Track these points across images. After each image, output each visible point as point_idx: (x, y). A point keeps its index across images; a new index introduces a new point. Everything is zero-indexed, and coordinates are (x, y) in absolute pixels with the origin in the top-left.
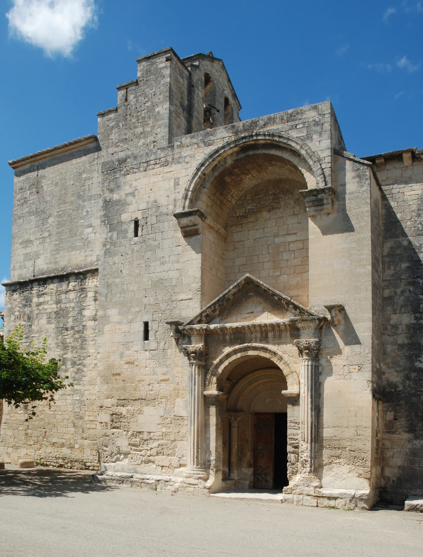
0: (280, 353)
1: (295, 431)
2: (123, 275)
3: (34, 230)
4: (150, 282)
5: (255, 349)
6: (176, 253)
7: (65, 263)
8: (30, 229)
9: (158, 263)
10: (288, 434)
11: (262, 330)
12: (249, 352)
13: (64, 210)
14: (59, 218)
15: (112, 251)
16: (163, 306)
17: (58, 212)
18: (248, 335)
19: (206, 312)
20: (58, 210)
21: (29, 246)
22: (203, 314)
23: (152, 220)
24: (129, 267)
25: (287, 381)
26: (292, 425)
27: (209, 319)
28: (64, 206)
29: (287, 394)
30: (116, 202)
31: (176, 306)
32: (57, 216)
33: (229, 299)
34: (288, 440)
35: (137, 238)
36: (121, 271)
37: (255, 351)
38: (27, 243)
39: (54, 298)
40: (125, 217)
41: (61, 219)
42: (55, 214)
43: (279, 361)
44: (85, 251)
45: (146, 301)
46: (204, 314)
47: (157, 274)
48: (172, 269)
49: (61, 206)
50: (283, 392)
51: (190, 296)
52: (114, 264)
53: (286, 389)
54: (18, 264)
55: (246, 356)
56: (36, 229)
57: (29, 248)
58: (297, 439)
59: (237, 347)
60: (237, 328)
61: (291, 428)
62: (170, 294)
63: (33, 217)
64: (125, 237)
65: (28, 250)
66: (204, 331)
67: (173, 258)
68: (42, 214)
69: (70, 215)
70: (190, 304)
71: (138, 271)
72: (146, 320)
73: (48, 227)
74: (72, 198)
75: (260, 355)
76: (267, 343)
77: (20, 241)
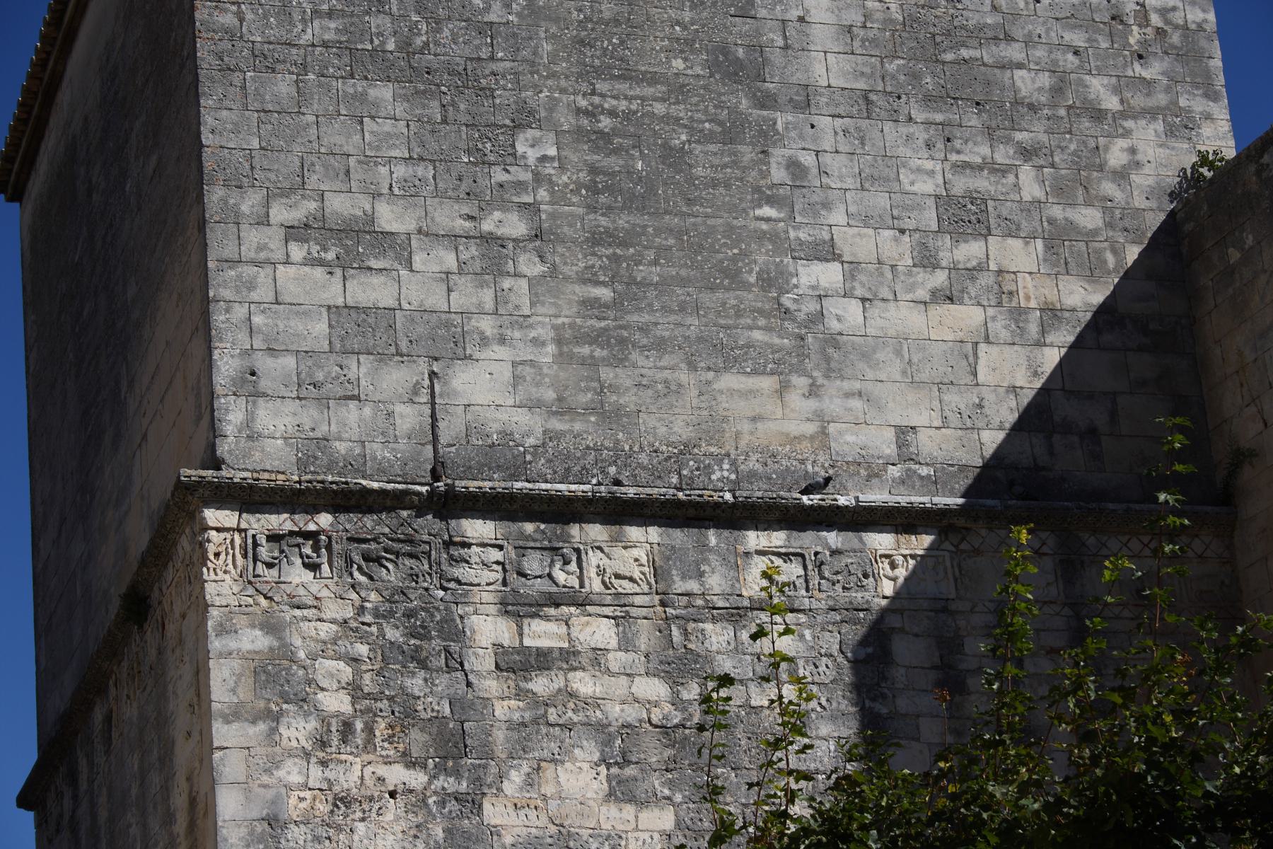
3: (401, 171)
8: (368, 161)
13: (629, 115)
14: (596, 149)
20: (583, 103)
21: (373, 263)
28: (623, 87)
32: (579, 132)
39: (646, 636)
41: (614, 163)
42: (566, 121)
49: (602, 86)
54: (290, 362)
57: (376, 280)
65: (372, 290)
73: (520, 186)
74: (678, 64)
77: (281, 213)
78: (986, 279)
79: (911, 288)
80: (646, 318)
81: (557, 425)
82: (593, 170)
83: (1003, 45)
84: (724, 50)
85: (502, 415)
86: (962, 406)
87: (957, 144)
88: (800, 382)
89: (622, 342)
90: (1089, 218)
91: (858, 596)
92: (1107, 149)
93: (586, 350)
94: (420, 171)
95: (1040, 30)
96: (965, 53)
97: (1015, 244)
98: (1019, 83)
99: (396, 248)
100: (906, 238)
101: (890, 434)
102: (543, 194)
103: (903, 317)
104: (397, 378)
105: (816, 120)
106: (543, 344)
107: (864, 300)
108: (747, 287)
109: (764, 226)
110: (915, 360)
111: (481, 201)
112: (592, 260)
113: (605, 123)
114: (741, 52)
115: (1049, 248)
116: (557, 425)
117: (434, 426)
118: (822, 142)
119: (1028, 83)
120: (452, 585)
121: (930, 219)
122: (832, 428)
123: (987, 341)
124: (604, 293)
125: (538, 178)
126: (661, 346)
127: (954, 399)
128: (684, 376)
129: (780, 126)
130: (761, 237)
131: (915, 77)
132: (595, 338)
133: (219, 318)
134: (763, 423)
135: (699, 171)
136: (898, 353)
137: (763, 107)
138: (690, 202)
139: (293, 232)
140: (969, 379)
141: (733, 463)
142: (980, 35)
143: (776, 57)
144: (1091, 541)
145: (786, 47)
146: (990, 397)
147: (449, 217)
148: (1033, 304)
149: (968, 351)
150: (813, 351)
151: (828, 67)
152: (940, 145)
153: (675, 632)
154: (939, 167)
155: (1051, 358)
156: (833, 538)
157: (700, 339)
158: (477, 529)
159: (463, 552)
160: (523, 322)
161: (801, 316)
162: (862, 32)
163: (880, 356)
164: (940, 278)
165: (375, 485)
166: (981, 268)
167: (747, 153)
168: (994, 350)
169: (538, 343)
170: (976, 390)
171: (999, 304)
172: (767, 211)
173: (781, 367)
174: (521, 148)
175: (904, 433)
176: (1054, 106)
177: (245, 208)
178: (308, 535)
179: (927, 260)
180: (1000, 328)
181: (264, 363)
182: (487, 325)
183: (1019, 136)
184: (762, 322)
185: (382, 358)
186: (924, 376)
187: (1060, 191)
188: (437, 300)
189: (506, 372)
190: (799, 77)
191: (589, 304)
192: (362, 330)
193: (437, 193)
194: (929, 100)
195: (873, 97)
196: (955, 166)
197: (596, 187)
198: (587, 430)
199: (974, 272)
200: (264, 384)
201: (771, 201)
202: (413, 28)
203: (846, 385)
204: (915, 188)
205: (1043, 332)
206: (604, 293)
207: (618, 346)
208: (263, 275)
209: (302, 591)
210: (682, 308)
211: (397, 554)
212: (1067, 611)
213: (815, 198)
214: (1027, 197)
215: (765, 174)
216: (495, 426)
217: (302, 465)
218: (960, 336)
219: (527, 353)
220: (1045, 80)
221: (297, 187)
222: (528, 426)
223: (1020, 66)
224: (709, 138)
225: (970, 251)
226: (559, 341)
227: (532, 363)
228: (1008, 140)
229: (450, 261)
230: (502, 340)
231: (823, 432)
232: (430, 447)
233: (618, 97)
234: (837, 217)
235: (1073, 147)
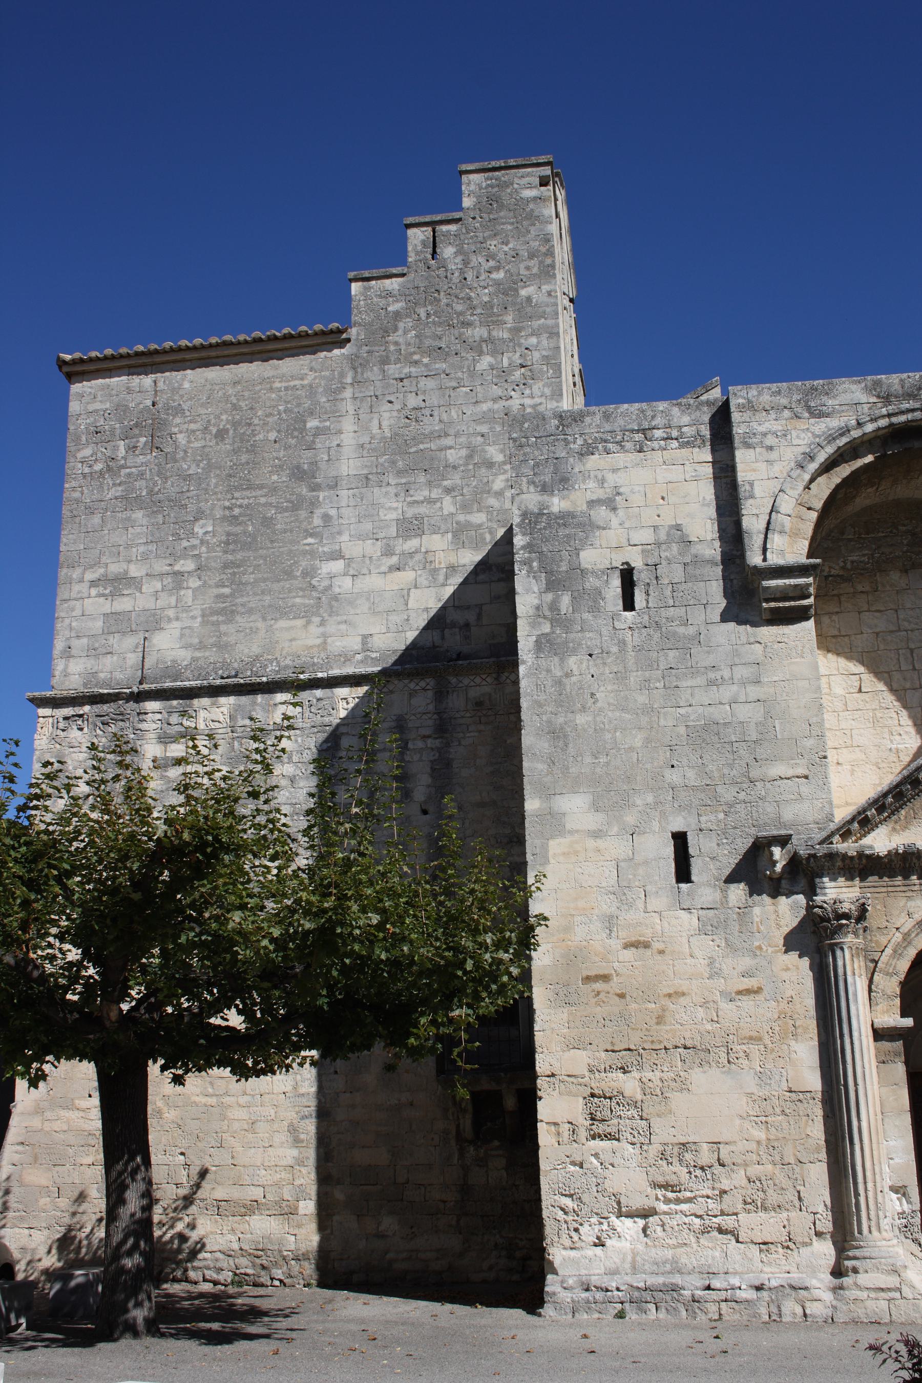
2: (599, 705)
3: (142, 549)
4: (682, 730)
6: (751, 660)
7: (256, 650)
8: (128, 547)
9: (700, 680)
13: (248, 506)
14: (231, 524)
15: (559, 640)
16: (727, 794)
17: (229, 508)
20: (227, 504)
21: (125, 592)
23: (673, 573)
24: (616, 687)
28: (247, 493)
30: (563, 518)
31: (763, 793)
32: (224, 518)
35: (633, 613)
36: (592, 694)
38: (117, 584)
40: (589, 557)
41: (239, 529)
42: (218, 513)
44: (322, 623)
45: (673, 777)
47: (700, 710)
48: (742, 698)
49: (237, 495)
51: (801, 771)
52: (568, 675)
54: (85, 641)
56: (153, 547)
57: (125, 599)
63: (139, 515)
64: (595, 609)
65: (123, 604)
66: (864, 861)
67: (741, 672)
68: (168, 509)
69: (268, 522)
71: (642, 699)
72: (678, 825)
73: (194, 547)
77: (90, 576)
78: (418, 557)
79: (378, 567)
80: (245, 599)
81: (198, 654)
82: (228, 534)
83: (443, 439)
84: (298, 467)
85: (173, 653)
86: (398, 621)
87: (411, 492)
88: (316, 620)
89: (232, 612)
90: (479, 518)
91: (326, 720)
92: (493, 481)
93: (215, 618)
94: (150, 547)
95: (464, 428)
96: (421, 446)
97: (436, 537)
98: (449, 456)
99: (135, 583)
100: (379, 543)
101: (359, 639)
102: (204, 549)
103: (374, 582)
104: (130, 641)
105: (339, 493)
106: (196, 618)
107: (353, 576)
108: (295, 578)
109: (307, 548)
110: (376, 602)
111: (175, 557)
112: (224, 576)
113: (237, 511)
114: (306, 467)
115: (454, 536)
116: (198, 654)
117: (143, 661)
118: (341, 505)
119: (452, 456)
120: (138, 732)
121: (393, 531)
122: (329, 640)
123: (416, 587)
124: (227, 591)
125: (202, 542)
126: (250, 611)
127: (395, 618)
128: (260, 624)
129: (321, 499)
130: (305, 553)
131: (394, 462)
132: (217, 613)
133: (58, 625)
134: (294, 642)
135: (279, 526)
136: (368, 599)
137: (314, 490)
138: (272, 542)
139: (93, 583)
140: (404, 607)
141: (278, 663)
142: (431, 437)
143: (323, 465)
144: (454, 680)
145: (329, 460)
146: (413, 615)
147: (161, 566)
148: (443, 565)
149: (404, 595)
150: (326, 604)
151: (349, 466)
152: (403, 494)
153: (236, 743)
154: (400, 505)
155: (449, 591)
156: (319, 693)
157: (270, 606)
158: (152, 706)
159: (144, 717)
160: (187, 609)
161: (321, 588)
162: (368, 446)
163: (358, 602)
164: (394, 560)
165: (106, 691)
166: (416, 552)
167: (303, 514)
168: (418, 591)
169: (194, 618)
170: (406, 612)
171: (424, 568)
172: (310, 540)
173: (307, 614)
174: (196, 530)
175: (365, 638)
176: (467, 464)
177: (74, 576)
178: (81, 716)
179: (388, 552)
180: (423, 581)
181: (75, 643)
182: (171, 613)
183: (445, 483)
184: (301, 593)
185: (124, 633)
186: (380, 609)
187: (465, 508)
188: (151, 605)
189: (177, 633)
190: (334, 473)
191: (218, 596)
192: (117, 623)
193: (157, 557)
194: (400, 473)
195: (370, 476)
196: (409, 503)
197: (230, 542)
198: (211, 655)
199: (411, 555)
200: (74, 652)
201: (312, 535)
202: (155, 484)
203: (339, 618)
204: (386, 518)
205: (446, 578)
206: (227, 591)
207: (229, 614)
208: (78, 604)
209: (74, 740)
210: (263, 593)
211: (116, 720)
212: (436, 716)
213: (335, 530)
214: (446, 512)
215: (310, 523)
216: (170, 658)
217: (85, 685)
218: (402, 586)
219: (188, 623)
220: (464, 452)
221: (97, 563)
222: (184, 656)
223: (450, 448)
224: (286, 510)
225: (413, 544)
226: (203, 616)
227: (189, 628)
228: (439, 486)
229: (159, 586)
230: (177, 619)
231: (325, 643)
232: (140, 671)
233: (243, 498)
234: (345, 537)
235: (474, 484)
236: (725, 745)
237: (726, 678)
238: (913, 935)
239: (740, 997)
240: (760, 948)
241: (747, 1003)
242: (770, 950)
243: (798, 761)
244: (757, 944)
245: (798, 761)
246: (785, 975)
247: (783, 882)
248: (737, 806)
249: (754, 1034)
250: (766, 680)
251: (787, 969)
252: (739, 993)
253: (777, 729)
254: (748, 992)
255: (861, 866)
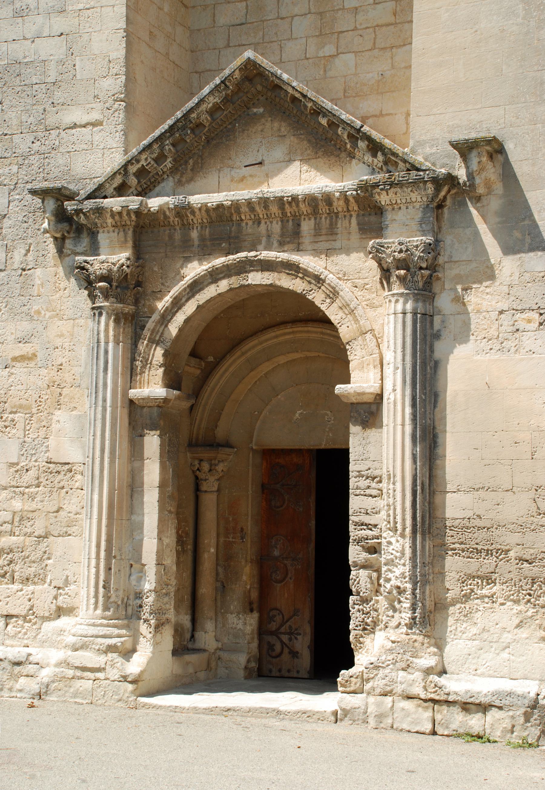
0: (331, 278)
1: (369, 503)
5: (267, 266)
10: (351, 512)
11: (284, 214)
12: (251, 275)
18: (249, 228)
19: (138, 161)
22: (130, 167)
25: (350, 358)
26: (363, 483)
27: (147, 185)
29: (347, 396)
31: (57, 143)
33: (199, 125)
34: (351, 527)
37: (266, 274)
43: (328, 301)
46: (133, 169)
50: (340, 388)
51: (95, 116)
53: (347, 380)
55: (242, 286)
58: (375, 526)
59: (219, 261)
60: (220, 206)
61: (358, 492)
62: (41, 108)
66: (133, 217)
70: (96, 138)
75: (278, 283)
76: (298, 249)
236: (25, 88)
237: (32, 7)
238: (184, 300)
239: (14, 364)
240: (38, 312)
241: (19, 370)
242: (48, 314)
243: (93, 105)
244: (36, 308)
245: (93, 105)
246: (58, 342)
247: (67, 241)
248: (32, 158)
249: (23, 402)
250: (71, 8)
251: (61, 336)
252: (15, 359)
253: (77, 67)
254: (23, 358)
255: (133, 223)
